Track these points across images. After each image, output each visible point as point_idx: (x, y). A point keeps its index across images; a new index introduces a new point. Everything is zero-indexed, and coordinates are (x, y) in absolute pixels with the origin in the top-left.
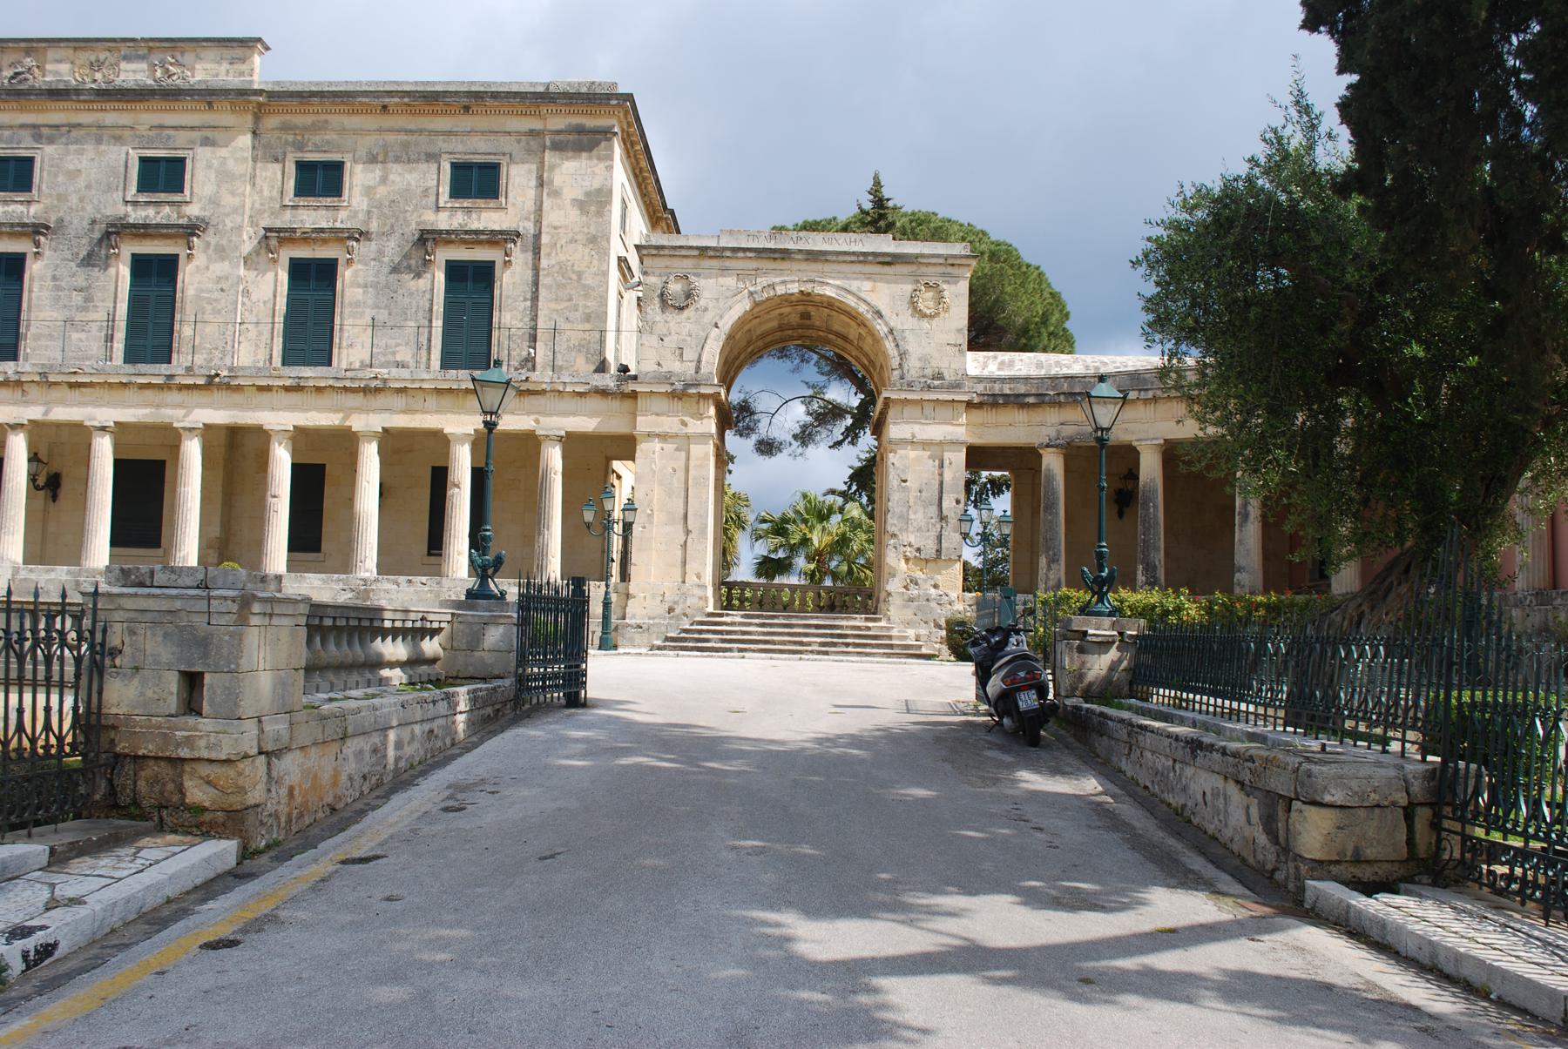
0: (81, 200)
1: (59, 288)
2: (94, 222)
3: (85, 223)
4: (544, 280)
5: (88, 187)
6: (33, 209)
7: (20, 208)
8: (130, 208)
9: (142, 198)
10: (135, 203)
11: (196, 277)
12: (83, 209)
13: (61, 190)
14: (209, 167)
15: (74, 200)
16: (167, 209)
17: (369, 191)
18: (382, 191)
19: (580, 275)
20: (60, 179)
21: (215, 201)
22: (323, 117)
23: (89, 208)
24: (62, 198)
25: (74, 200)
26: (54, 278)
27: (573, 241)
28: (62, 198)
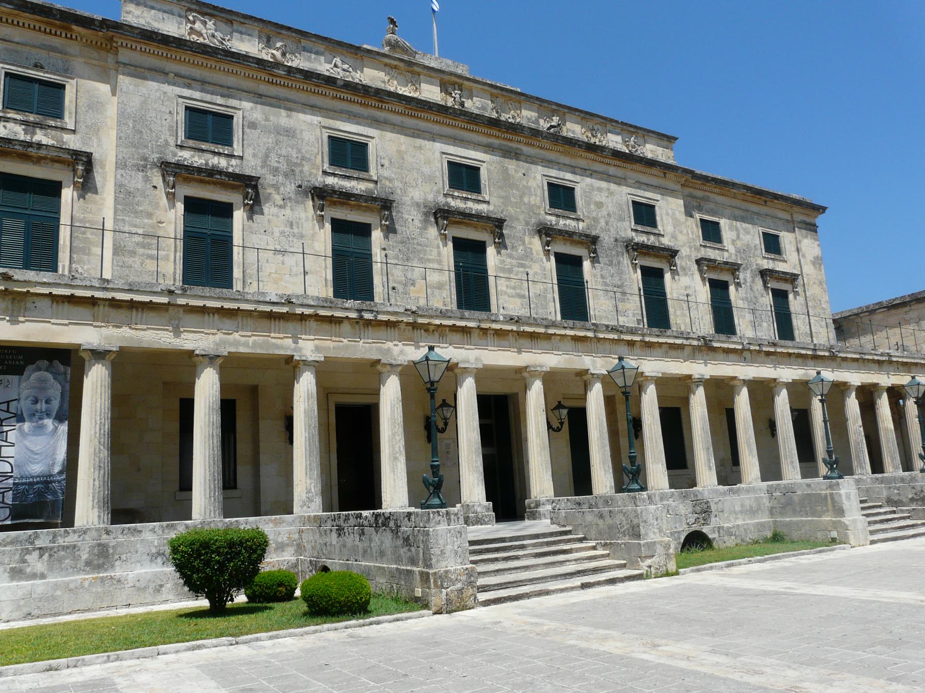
0: (607, 223)
1: (606, 284)
2: (616, 240)
3: (612, 240)
4: (810, 304)
5: (609, 215)
6: (581, 225)
7: (573, 223)
8: (634, 234)
9: (639, 228)
10: (636, 231)
11: (672, 286)
12: (609, 230)
13: (594, 214)
14: (667, 214)
15: (602, 223)
16: (652, 238)
17: (733, 242)
18: (739, 244)
19: (820, 301)
20: (592, 206)
21: (674, 237)
22: (707, 194)
23: (612, 229)
24: (596, 220)
25: (602, 223)
26: (602, 277)
27: (815, 283)
28: (596, 220)
